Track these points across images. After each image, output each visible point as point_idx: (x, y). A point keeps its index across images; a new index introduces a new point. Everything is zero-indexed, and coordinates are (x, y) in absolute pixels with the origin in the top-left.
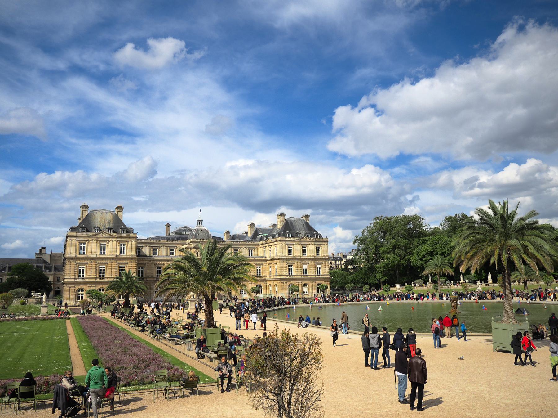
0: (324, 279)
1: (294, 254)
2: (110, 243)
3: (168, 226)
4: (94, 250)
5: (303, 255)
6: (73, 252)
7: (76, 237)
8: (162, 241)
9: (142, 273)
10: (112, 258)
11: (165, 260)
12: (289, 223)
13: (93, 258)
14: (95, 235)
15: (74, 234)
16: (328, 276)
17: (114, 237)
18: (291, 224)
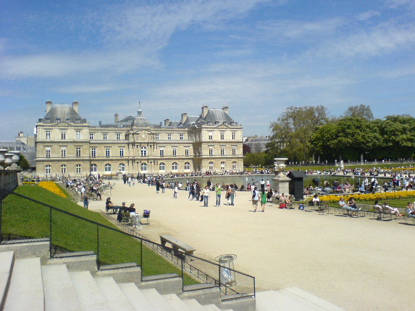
0: (238, 158)
1: (214, 139)
3: (116, 115)
7: (43, 126)
8: (110, 128)
9: (95, 154)
10: (71, 142)
11: (112, 143)
12: (211, 114)
13: (56, 142)
15: (41, 124)
16: (242, 156)
17: (71, 126)
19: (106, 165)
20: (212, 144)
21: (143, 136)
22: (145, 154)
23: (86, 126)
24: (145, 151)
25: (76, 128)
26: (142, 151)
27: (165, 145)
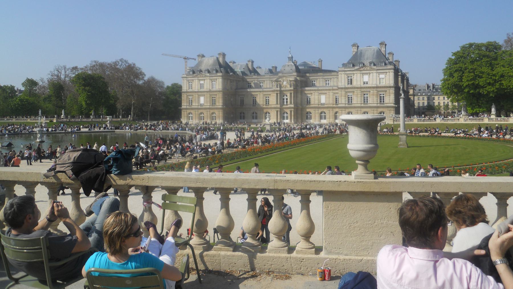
0: (388, 107)
2: (206, 81)
4: (197, 86)
5: (364, 83)
6: (343, 84)
10: (207, 92)
12: (359, 53)
13: (195, 92)
14: (196, 76)
16: (393, 105)
18: (361, 53)
19: (253, 113)
20: (351, 90)
21: (285, 83)
22: (287, 102)
23: (219, 76)
24: (287, 99)
25: (211, 78)
26: (284, 99)
27: (311, 92)
